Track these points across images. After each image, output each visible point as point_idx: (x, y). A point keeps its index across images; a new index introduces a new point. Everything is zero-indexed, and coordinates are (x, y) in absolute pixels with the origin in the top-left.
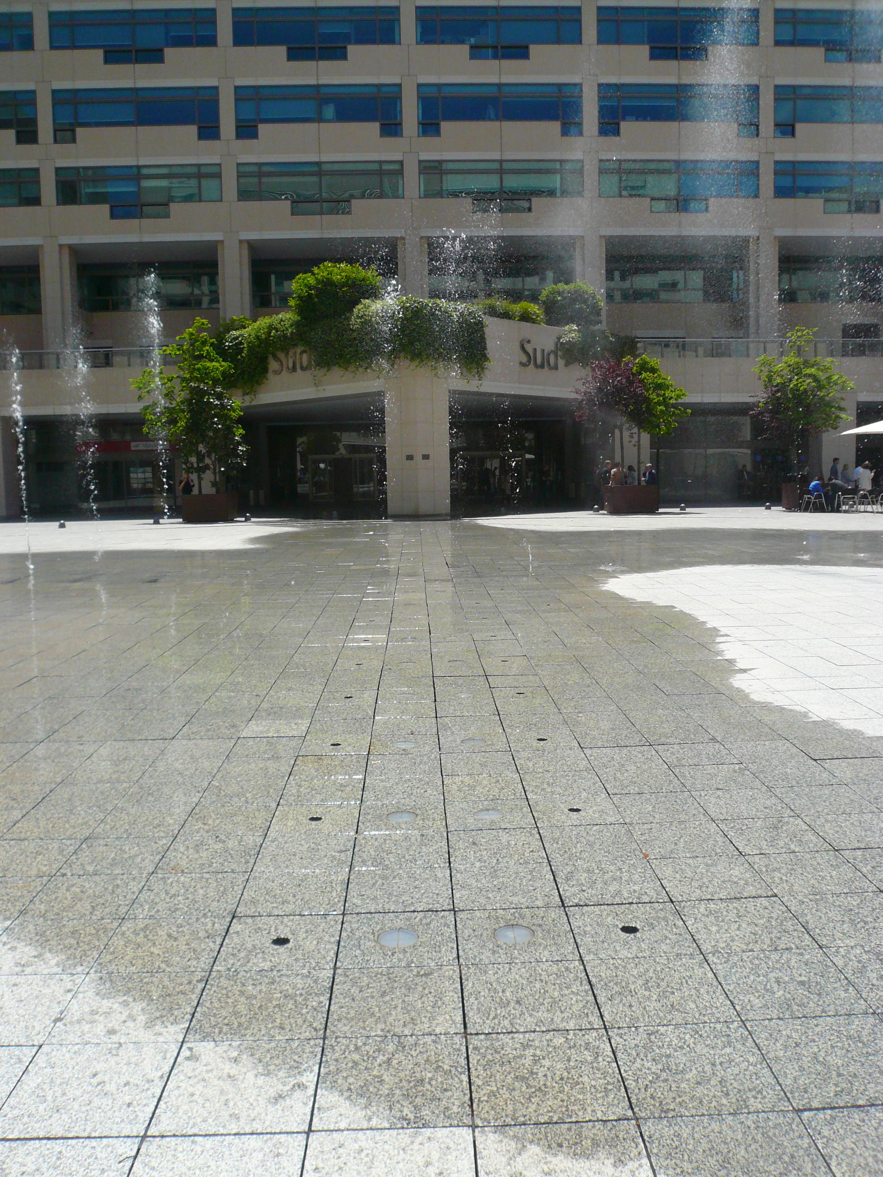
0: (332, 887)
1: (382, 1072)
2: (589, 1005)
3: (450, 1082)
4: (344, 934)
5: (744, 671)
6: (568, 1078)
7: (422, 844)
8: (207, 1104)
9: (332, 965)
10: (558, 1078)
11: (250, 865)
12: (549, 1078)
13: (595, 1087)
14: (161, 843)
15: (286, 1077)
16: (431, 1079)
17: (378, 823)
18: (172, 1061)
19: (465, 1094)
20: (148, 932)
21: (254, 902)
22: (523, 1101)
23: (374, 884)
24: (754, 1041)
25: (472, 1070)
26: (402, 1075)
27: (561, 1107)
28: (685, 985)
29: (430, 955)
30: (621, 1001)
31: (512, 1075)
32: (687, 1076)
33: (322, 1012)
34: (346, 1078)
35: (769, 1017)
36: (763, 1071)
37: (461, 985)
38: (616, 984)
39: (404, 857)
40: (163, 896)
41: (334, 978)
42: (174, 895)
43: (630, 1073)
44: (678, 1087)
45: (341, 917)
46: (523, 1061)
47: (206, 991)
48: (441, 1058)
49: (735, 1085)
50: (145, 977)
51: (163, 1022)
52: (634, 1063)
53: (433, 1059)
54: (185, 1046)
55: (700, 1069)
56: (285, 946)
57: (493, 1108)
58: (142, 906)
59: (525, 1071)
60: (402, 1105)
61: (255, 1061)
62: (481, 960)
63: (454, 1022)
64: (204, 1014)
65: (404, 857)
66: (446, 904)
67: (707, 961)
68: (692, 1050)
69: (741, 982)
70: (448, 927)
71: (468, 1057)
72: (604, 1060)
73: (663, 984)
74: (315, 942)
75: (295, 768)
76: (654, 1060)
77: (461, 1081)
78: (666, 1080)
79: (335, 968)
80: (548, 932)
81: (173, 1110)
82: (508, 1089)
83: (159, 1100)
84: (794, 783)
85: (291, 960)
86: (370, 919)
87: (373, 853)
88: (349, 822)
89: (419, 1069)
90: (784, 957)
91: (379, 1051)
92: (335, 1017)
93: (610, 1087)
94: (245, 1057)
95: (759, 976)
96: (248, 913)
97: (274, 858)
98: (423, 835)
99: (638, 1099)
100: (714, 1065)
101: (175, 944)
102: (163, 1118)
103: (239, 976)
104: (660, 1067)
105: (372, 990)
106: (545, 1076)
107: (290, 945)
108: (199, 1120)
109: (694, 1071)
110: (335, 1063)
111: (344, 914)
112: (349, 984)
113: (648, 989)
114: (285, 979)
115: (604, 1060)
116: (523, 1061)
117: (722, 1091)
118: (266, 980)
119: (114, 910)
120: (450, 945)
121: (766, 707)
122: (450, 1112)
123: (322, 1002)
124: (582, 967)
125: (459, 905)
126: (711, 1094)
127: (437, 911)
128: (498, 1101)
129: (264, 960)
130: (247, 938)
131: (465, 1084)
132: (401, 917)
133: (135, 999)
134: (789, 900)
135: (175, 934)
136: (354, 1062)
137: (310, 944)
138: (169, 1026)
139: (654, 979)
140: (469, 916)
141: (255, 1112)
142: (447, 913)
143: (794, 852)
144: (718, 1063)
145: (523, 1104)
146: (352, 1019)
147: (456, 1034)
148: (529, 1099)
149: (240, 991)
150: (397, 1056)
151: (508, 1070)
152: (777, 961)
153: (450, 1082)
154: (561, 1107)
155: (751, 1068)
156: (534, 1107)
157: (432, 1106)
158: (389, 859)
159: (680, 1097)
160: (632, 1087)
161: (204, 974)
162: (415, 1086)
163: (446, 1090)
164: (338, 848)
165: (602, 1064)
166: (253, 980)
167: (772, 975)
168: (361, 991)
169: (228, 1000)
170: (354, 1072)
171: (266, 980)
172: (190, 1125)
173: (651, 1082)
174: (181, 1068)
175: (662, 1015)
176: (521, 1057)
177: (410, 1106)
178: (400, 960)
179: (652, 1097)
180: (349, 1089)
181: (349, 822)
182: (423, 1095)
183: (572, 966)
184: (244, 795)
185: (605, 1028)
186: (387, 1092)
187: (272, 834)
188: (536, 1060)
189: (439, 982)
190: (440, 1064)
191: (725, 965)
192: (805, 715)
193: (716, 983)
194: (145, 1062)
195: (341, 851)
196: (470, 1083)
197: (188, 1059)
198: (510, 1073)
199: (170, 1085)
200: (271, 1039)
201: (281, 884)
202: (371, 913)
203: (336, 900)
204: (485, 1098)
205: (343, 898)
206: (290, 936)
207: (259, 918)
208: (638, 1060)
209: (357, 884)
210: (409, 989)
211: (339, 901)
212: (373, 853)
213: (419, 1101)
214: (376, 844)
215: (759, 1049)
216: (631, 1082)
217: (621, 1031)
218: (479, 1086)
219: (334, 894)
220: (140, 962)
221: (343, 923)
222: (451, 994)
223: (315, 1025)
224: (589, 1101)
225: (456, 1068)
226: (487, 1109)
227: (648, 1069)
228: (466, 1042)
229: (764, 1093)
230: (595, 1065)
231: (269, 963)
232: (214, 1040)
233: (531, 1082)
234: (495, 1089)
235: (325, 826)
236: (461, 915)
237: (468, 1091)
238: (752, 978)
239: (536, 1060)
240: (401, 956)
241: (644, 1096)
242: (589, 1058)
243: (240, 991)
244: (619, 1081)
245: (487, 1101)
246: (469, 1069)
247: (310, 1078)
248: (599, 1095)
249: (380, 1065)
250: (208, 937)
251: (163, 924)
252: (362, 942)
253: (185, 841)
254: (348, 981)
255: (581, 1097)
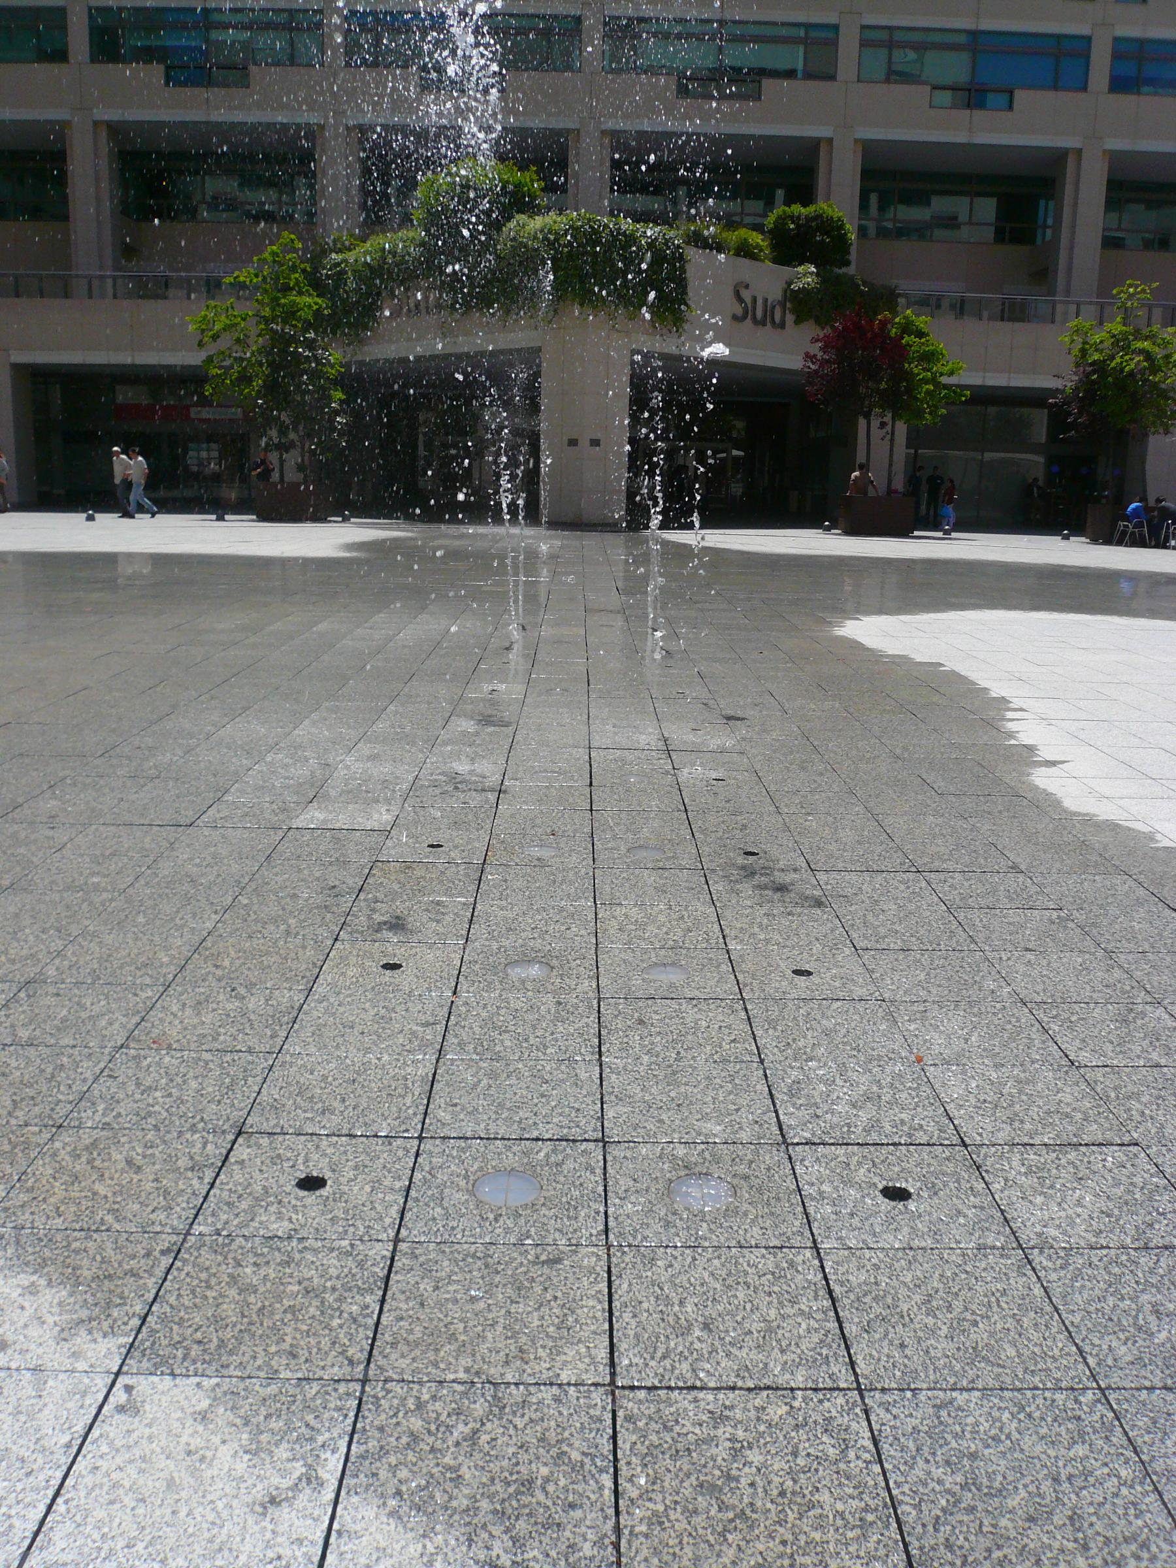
0: (407, 1088)
1: (461, 1458)
2: (829, 1340)
3: (579, 1488)
4: (418, 1176)
5: (1053, 764)
6: (793, 1493)
7: (557, 1019)
8: (140, 1511)
9: (392, 1234)
10: (775, 1492)
11: (279, 1041)
12: (760, 1490)
13: (842, 1515)
14: (144, 995)
15: (289, 1460)
16: (547, 1480)
17: (489, 978)
18: (94, 1413)
19: (606, 1518)
20: (95, 1154)
21: (277, 1107)
22: (711, 1538)
23: (475, 1086)
24: (1126, 1433)
25: (622, 1464)
26: (494, 1467)
27: (781, 1556)
28: (995, 1309)
29: (559, 1226)
30: (886, 1335)
31: (693, 1478)
32: (1011, 1503)
33: (366, 1327)
34: (393, 1469)
35: (1147, 1384)
36: (1147, 1500)
37: (610, 1287)
38: (876, 1299)
39: (526, 1040)
40: (131, 1087)
41: (392, 1259)
42: (150, 1088)
43: (906, 1488)
44: (995, 1526)
45: (416, 1142)
46: (714, 1451)
47: (174, 1272)
48: (566, 1434)
49: (1099, 1527)
50: (76, 1240)
51: (90, 1332)
52: (912, 1468)
53: (552, 1436)
54: (123, 1380)
55: (1032, 1488)
56: (318, 1193)
57: (656, 1552)
58: (93, 1104)
59: (717, 1473)
60: (492, 1536)
61: (238, 1421)
62: (645, 1238)
63: (593, 1361)
64: (163, 1319)
65: (526, 1040)
66: (590, 1128)
67: (1030, 1263)
68: (1016, 1446)
69: (1092, 1309)
70: (593, 1172)
71: (614, 1437)
72: (858, 1458)
73: (958, 1305)
74: (368, 1188)
75: (370, 880)
76: (948, 1463)
77: (601, 1488)
78: (971, 1510)
79: (397, 1240)
80: (760, 1191)
81: (78, 1518)
82: (685, 1510)
83: (57, 1494)
84: (1147, 947)
85: (323, 1220)
86: (463, 1150)
87: (477, 1030)
88: (445, 974)
89: (526, 1457)
90: (1163, 1263)
91: (458, 1413)
92: (388, 1338)
93: (870, 1517)
94: (221, 1410)
95: (1122, 1299)
96: (265, 1127)
97: (318, 1032)
98: (559, 1003)
99: (921, 1548)
100: (1056, 1480)
101: (136, 1178)
102: (56, 1536)
103: (233, 1247)
104: (959, 1478)
105: (455, 1287)
106: (752, 1485)
107: (324, 1192)
108: (121, 1543)
109: (1023, 1493)
110: (377, 1434)
111: (420, 1138)
112: (418, 1272)
113: (930, 1313)
114: (309, 1256)
115: (858, 1458)
116: (714, 1451)
117: (1076, 1541)
118: (278, 1257)
119: (47, 1111)
120: (594, 1206)
121: (1088, 821)
122: (577, 1555)
123: (367, 1307)
124: (816, 1262)
125: (614, 1134)
126: (1056, 1545)
127: (574, 1141)
128: (665, 1535)
129: (280, 1217)
130: (257, 1175)
131: (608, 1494)
132: (515, 1148)
133: (50, 1283)
134: (1159, 1152)
135: (139, 1160)
136: (412, 1434)
137: (359, 1192)
138: (100, 1340)
139: (941, 1293)
140: (629, 1154)
141: (225, 1531)
142: (591, 1145)
143: (1158, 1066)
144: (1063, 1477)
145: (711, 1545)
146: (417, 1344)
147: (596, 1385)
148: (722, 1534)
149: (231, 1276)
150: (489, 1426)
151: (686, 1467)
152: (1152, 1271)
153: (579, 1488)
154: (781, 1556)
155: (1124, 1491)
156: (731, 1552)
157: (546, 1540)
158: (502, 1041)
159: (999, 1547)
160: (910, 1519)
161: (174, 1238)
162: (518, 1492)
163: (572, 1506)
164: (423, 1018)
165: (856, 1466)
166: (256, 1255)
167: (1145, 1298)
168: (437, 1288)
169: (211, 1294)
170: (411, 1456)
171: (278, 1257)
172: (103, 1555)
173: (943, 1510)
174: (106, 1427)
175: (958, 1367)
176: (710, 1440)
177: (505, 1537)
178: (508, 1231)
179: (949, 1546)
180: (399, 1493)
181: (445, 974)
182: (530, 1515)
183: (800, 1259)
184: (285, 922)
185: (859, 1389)
186: (465, 1502)
187: (320, 989)
188: (737, 1451)
189: (571, 1280)
190: (565, 1448)
191: (1062, 1273)
192: (1150, 837)
193: (1049, 1309)
194: (46, 1412)
195: (427, 1024)
196: (616, 1492)
197: (121, 1409)
198: (688, 1475)
199: (81, 1465)
200: (273, 1376)
201: (325, 1077)
202: (467, 1138)
203: (411, 1111)
204: (643, 1528)
205: (422, 1108)
206: (327, 1175)
207: (281, 1138)
208: (920, 1462)
209: (447, 1084)
210: (519, 1289)
211: (415, 1114)
212: (477, 1030)
213: (522, 1526)
214: (484, 1014)
215: (1136, 1452)
216: (908, 1508)
217: (888, 1398)
218: (632, 1500)
219: (408, 1101)
220: (73, 1209)
221: (417, 1155)
222: (591, 1303)
223: (351, 1352)
224: (831, 1546)
225: (593, 1457)
226: (645, 1552)
227: (940, 1482)
228: (614, 1401)
229: (1154, 1548)
230: (842, 1466)
231: (286, 1223)
232: (173, 1374)
233: (728, 1499)
234: (661, 1508)
235: (405, 979)
236: (615, 1151)
237: (611, 1511)
238: (1111, 1301)
239: (737, 1451)
240: (510, 1223)
241: (932, 1542)
242: (831, 1451)
243: (231, 1276)
244: (885, 1505)
245: (646, 1536)
246: (616, 1459)
247: (332, 1464)
248: (850, 1535)
249: (457, 1444)
250: (192, 1168)
251: (123, 1140)
252: (446, 1191)
253: (181, 994)
254: (417, 1267)
255: (817, 1536)
